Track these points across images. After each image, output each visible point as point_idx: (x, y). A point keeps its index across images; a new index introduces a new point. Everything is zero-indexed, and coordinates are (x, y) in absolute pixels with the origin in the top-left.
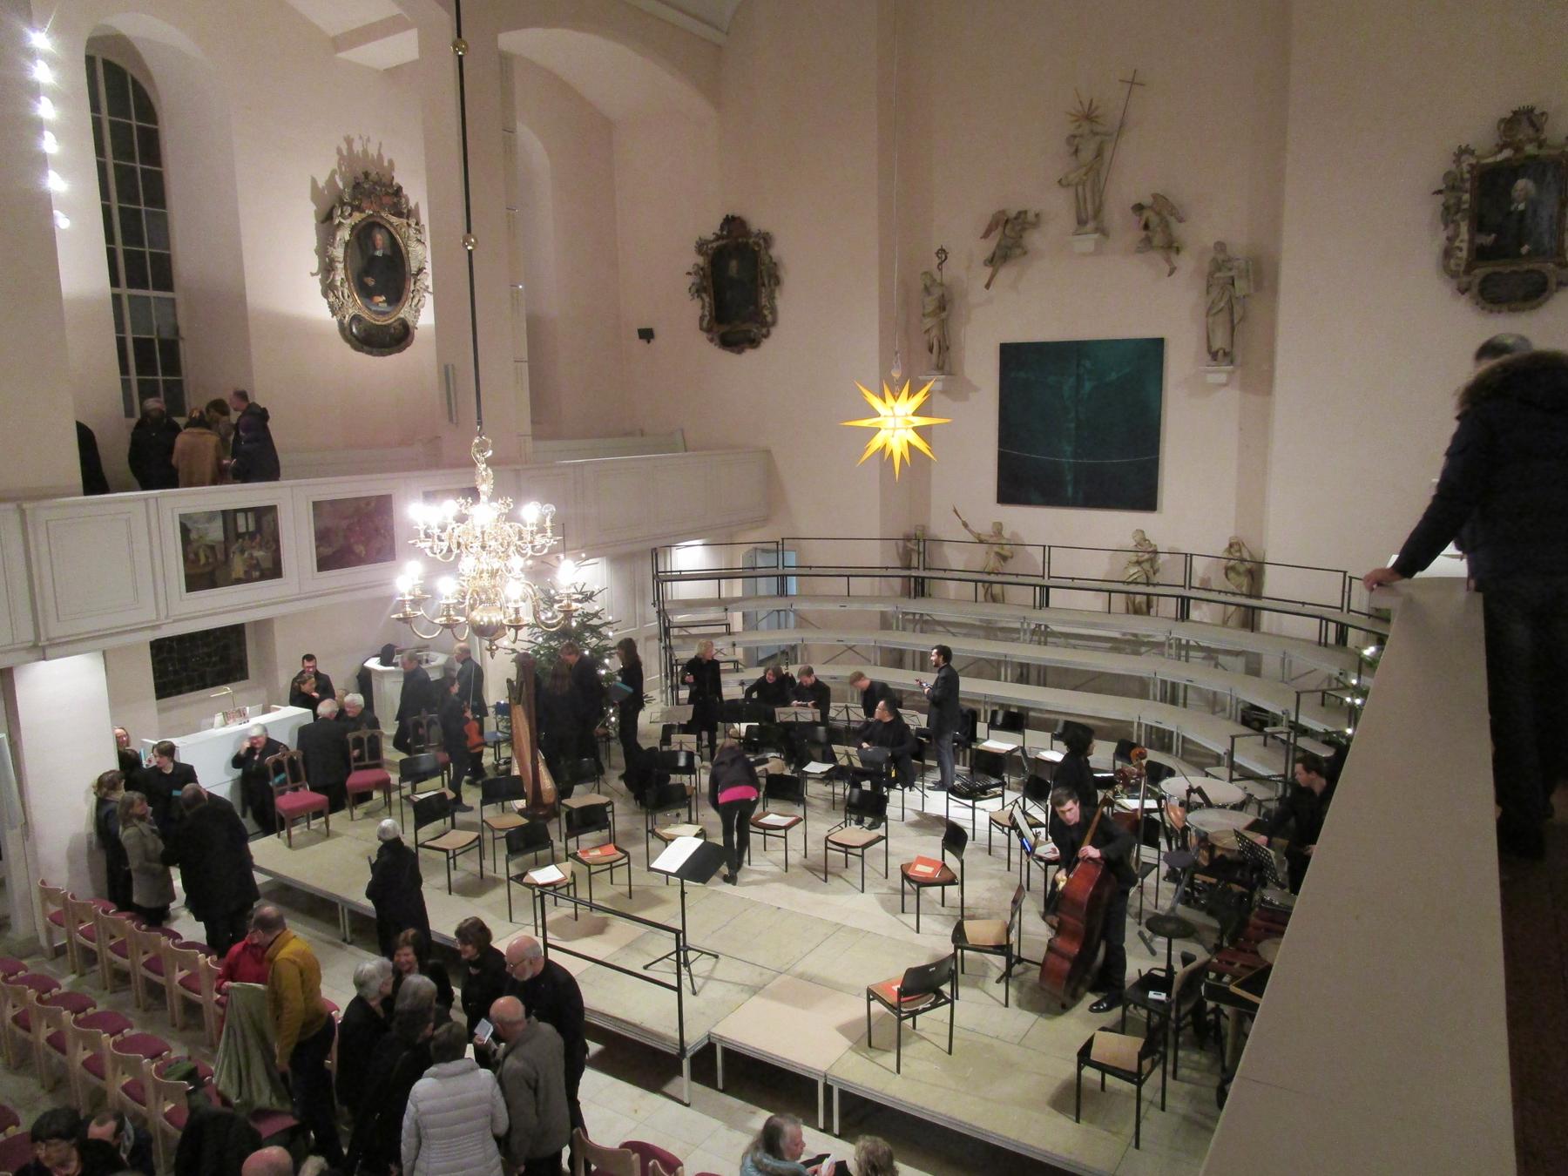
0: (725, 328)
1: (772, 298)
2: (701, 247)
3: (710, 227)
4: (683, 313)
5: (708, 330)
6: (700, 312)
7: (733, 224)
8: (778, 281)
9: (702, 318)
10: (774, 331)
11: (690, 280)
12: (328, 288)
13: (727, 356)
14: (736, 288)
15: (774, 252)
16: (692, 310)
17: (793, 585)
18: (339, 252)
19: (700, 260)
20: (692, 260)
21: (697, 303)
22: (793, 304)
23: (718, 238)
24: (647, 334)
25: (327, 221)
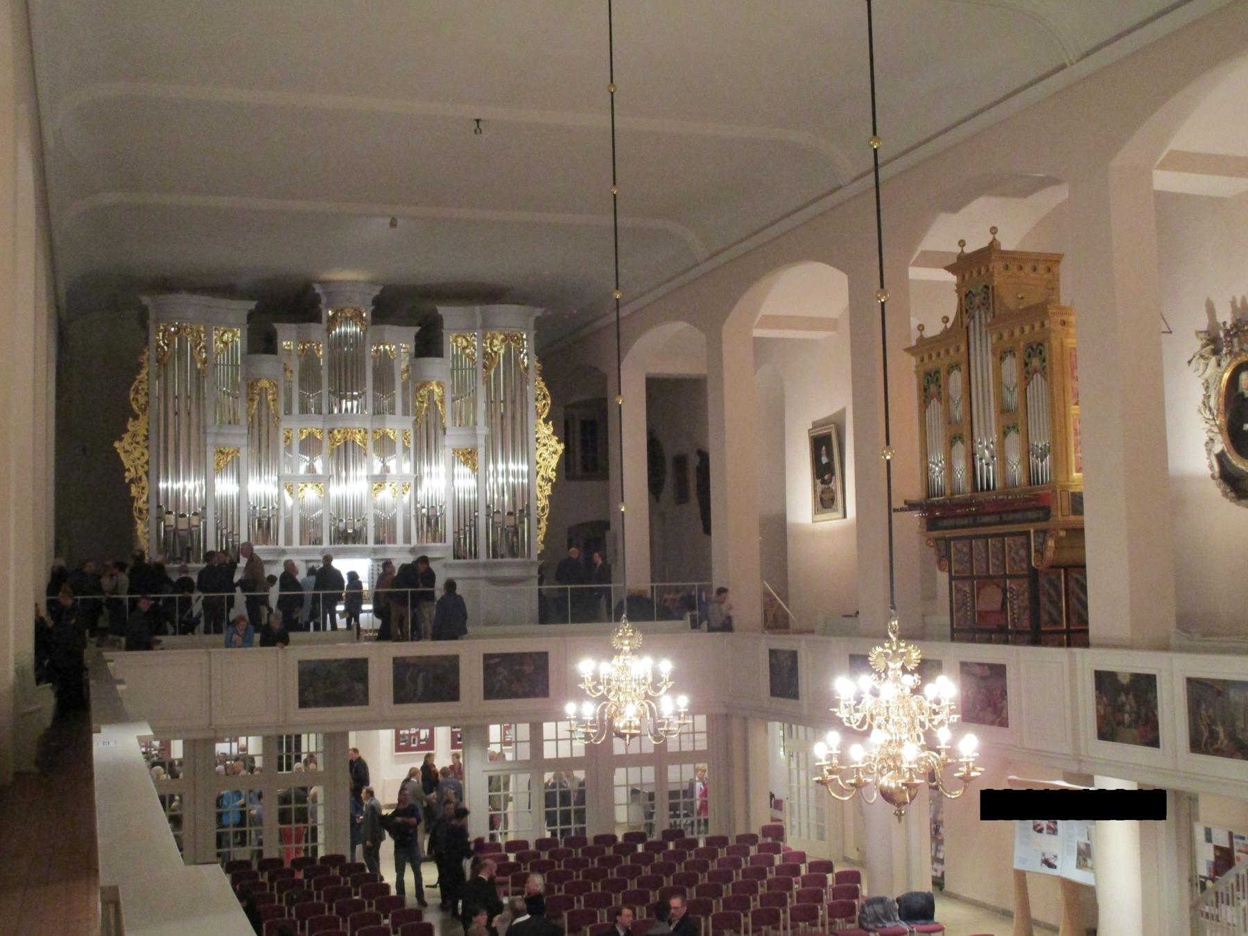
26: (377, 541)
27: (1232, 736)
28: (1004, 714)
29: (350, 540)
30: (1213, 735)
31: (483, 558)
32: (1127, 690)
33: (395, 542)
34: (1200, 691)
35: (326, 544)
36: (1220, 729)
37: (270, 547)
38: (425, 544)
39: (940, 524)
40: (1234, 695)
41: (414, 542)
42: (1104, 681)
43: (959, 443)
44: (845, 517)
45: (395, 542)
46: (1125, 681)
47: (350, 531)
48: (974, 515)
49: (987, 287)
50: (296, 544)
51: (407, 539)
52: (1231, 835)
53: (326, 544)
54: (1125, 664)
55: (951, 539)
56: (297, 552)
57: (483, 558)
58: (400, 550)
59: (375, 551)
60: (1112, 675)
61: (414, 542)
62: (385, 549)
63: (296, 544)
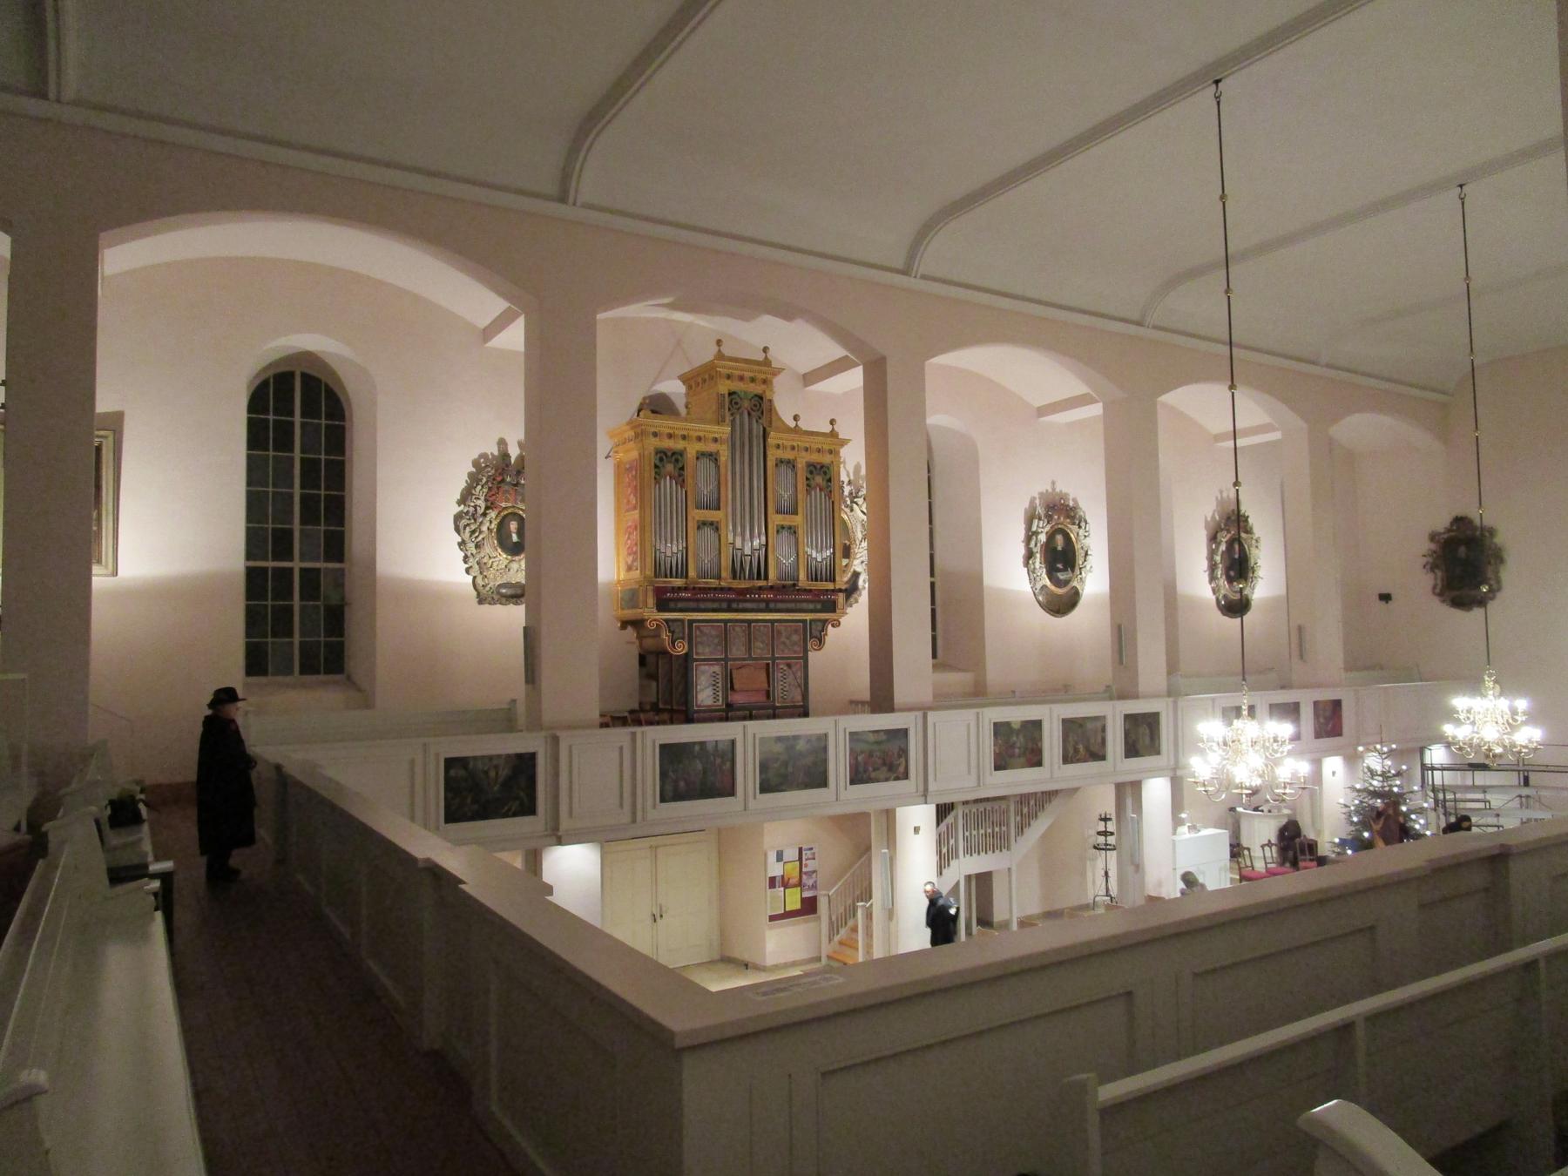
0: (1456, 593)
1: (1497, 572)
2: (1433, 537)
3: (1441, 522)
4: (1417, 584)
5: (1440, 595)
6: (1431, 583)
7: (1460, 521)
8: (1501, 560)
9: (1434, 587)
10: (1498, 595)
11: (1425, 560)
12: (1212, 578)
13: (1458, 614)
14: (1464, 564)
15: (1498, 540)
16: (1425, 582)
17: (1533, 778)
18: (1218, 558)
19: (1433, 546)
20: (1426, 546)
21: (1431, 576)
22: (1513, 576)
23: (1449, 530)
24: (1385, 598)
25: (1213, 538)
27: (1087, 749)
28: (901, 769)
30: (1076, 751)
32: (1018, 732)
34: (1069, 725)
36: (1081, 747)
39: (672, 605)
40: (1089, 725)
42: (1001, 729)
43: (708, 531)
44: (115, 573)
46: (1016, 727)
48: (730, 601)
49: (761, 398)
52: (800, 850)
54: (1016, 715)
55: (691, 622)
60: (1008, 724)
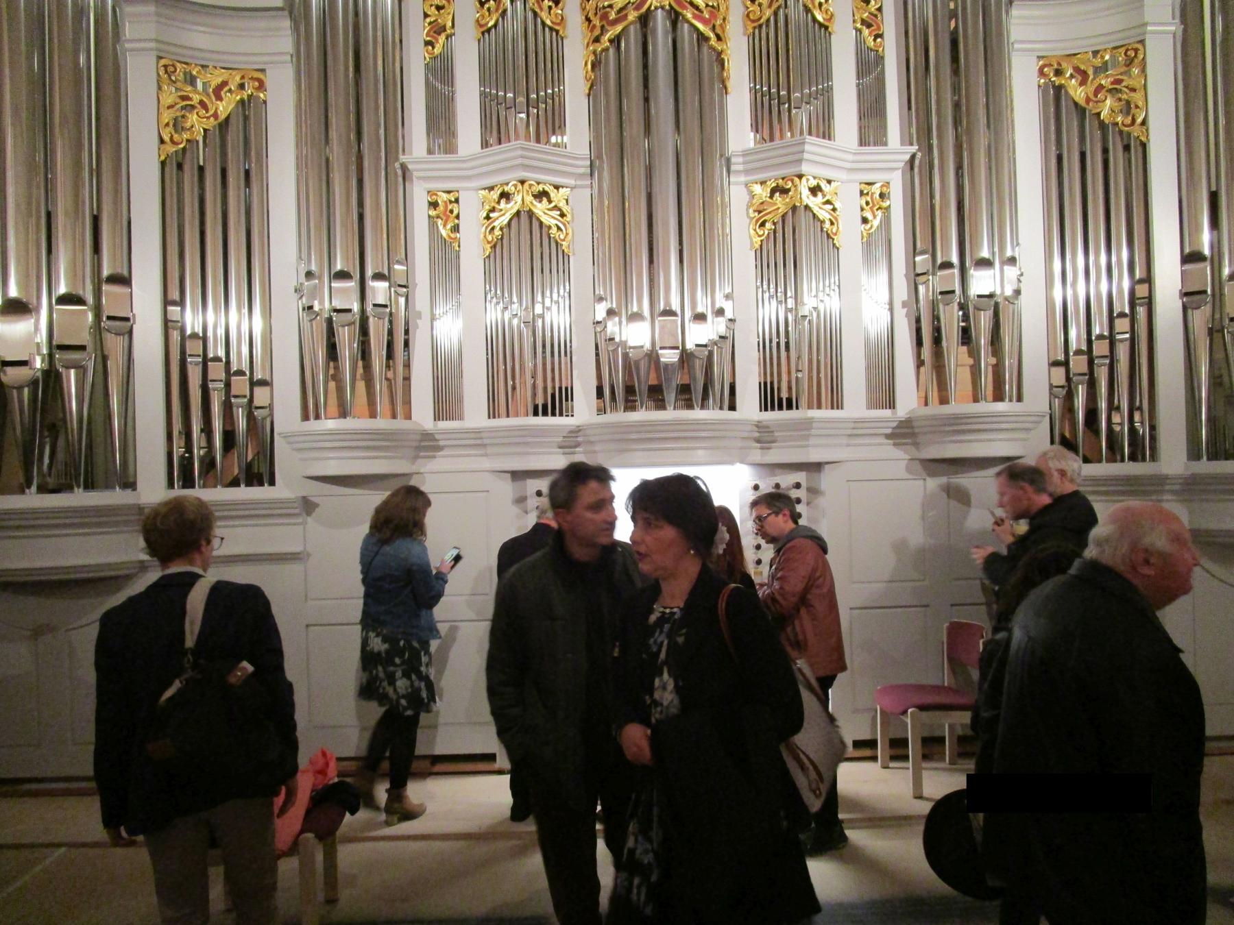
26: (771, 399)
29: (670, 396)
31: (1173, 458)
33: (837, 404)
35: (584, 408)
37: (382, 423)
38: (951, 409)
41: (908, 400)
45: (837, 404)
47: (669, 357)
50: (475, 413)
51: (884, 394)
53: (584, 408)
56: (478, 441)
57: (1173, 458)
58: (857, 430)
59: (764, 436)
61: (908, 400)
62: (808, 424)
63: (475, 413)
